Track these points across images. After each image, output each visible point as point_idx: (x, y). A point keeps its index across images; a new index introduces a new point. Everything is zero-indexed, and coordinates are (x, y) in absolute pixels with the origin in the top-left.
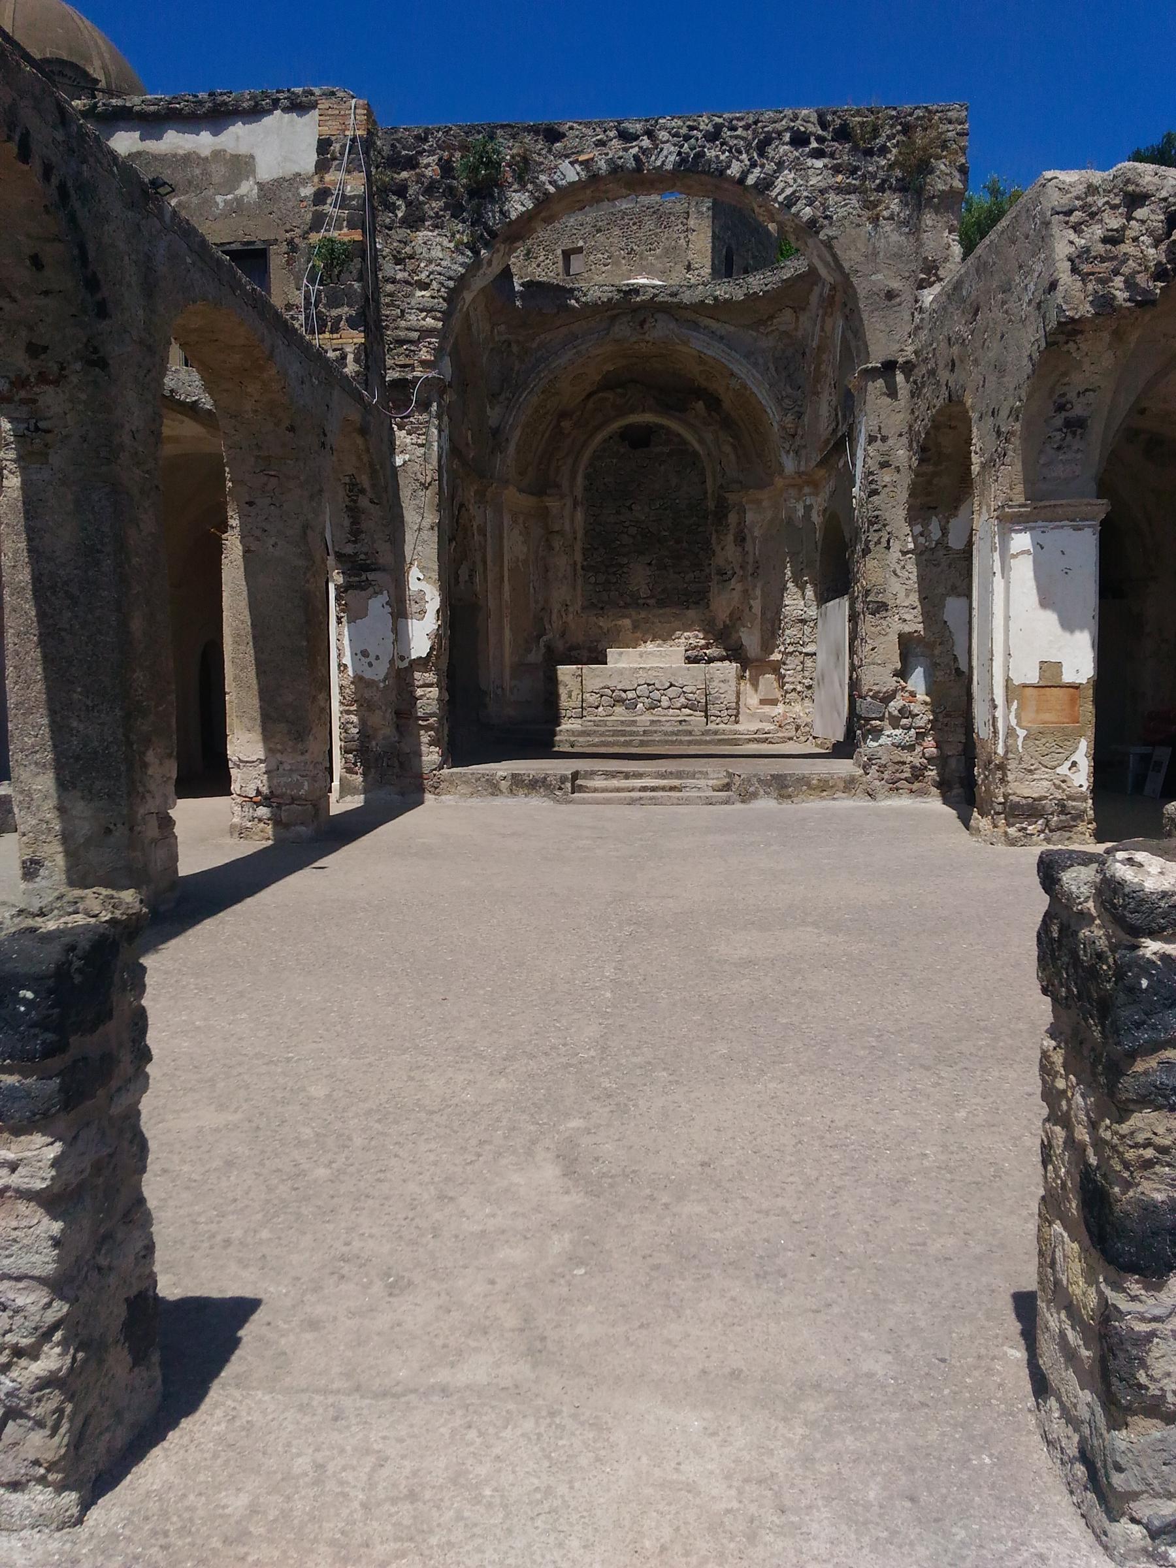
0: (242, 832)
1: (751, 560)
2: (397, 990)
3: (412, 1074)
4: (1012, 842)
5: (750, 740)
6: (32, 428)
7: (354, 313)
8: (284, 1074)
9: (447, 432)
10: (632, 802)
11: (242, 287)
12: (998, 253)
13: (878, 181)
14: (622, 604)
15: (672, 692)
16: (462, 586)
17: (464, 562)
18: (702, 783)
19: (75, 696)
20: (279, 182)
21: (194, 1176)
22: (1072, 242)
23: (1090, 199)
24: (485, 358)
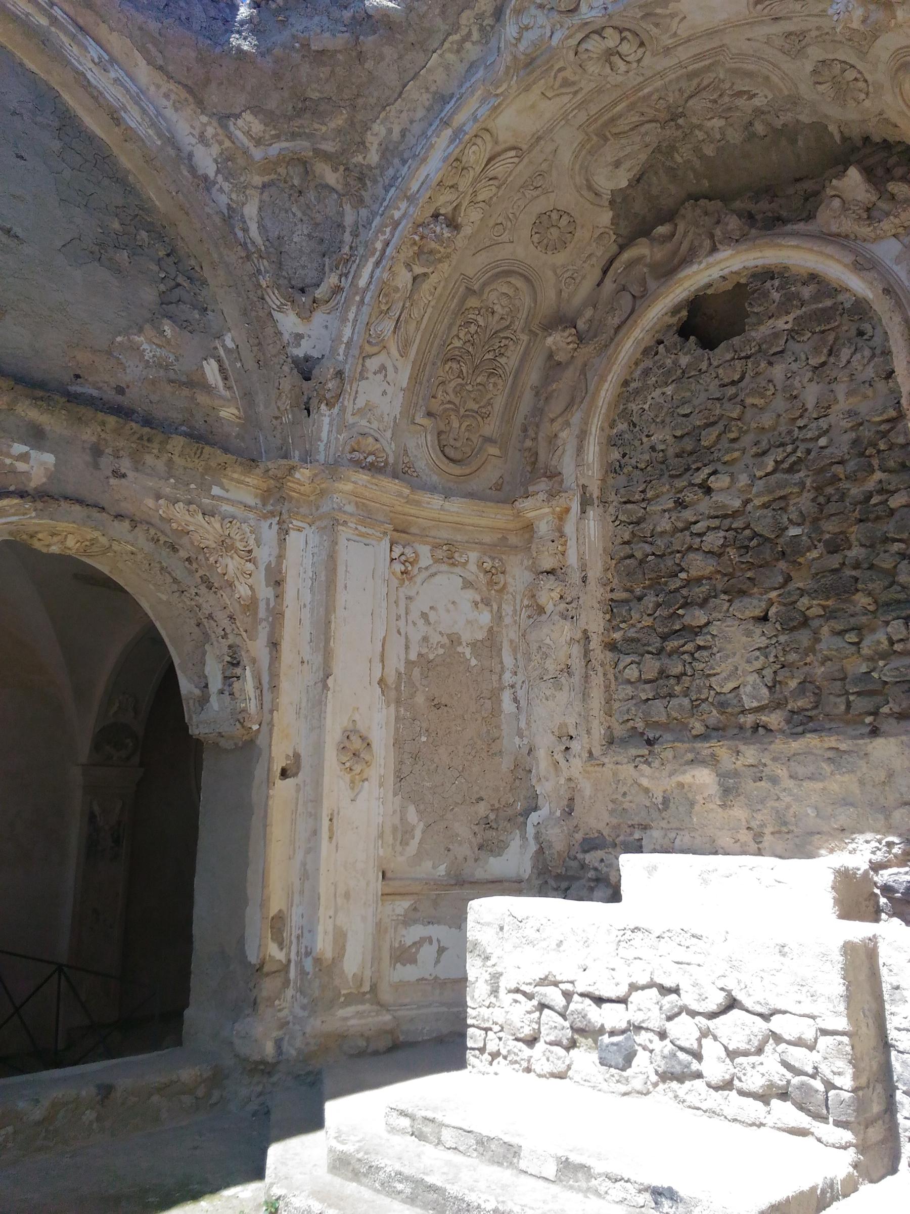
14: (699, 728)
17: (207, 647)
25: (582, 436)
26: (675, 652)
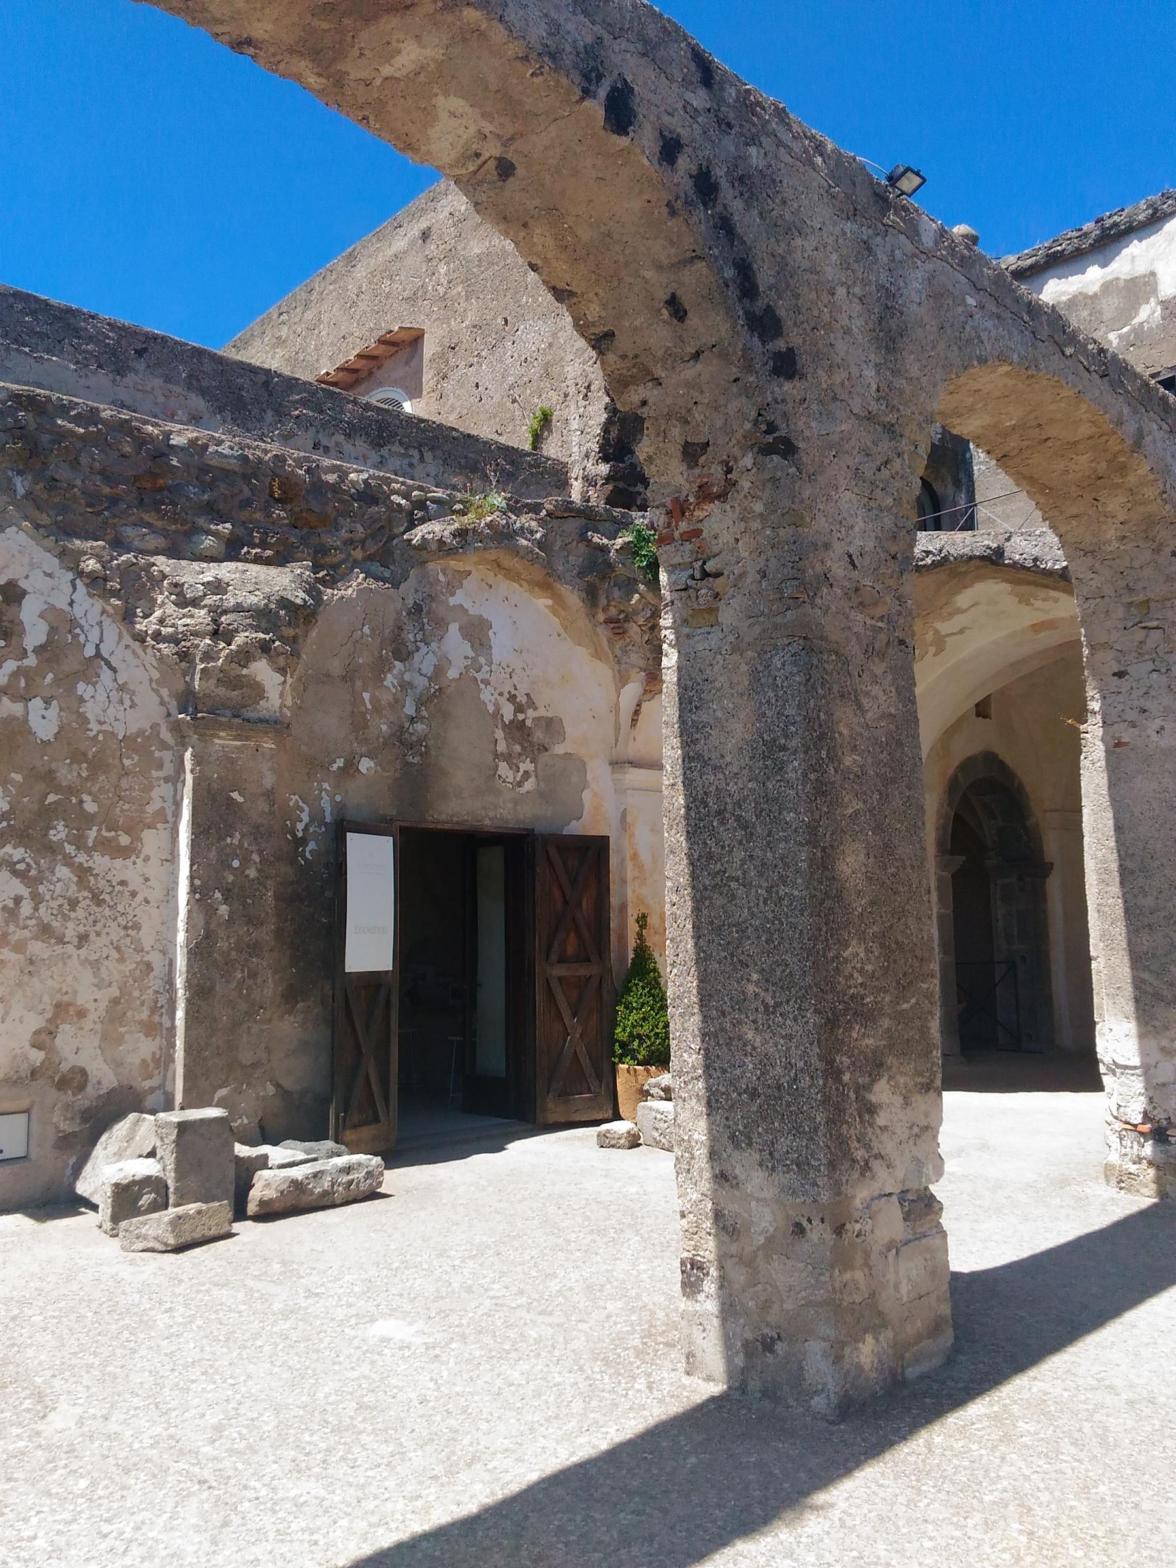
0: (1123, 1180)
6: (698, 575)
19: (751, 988)
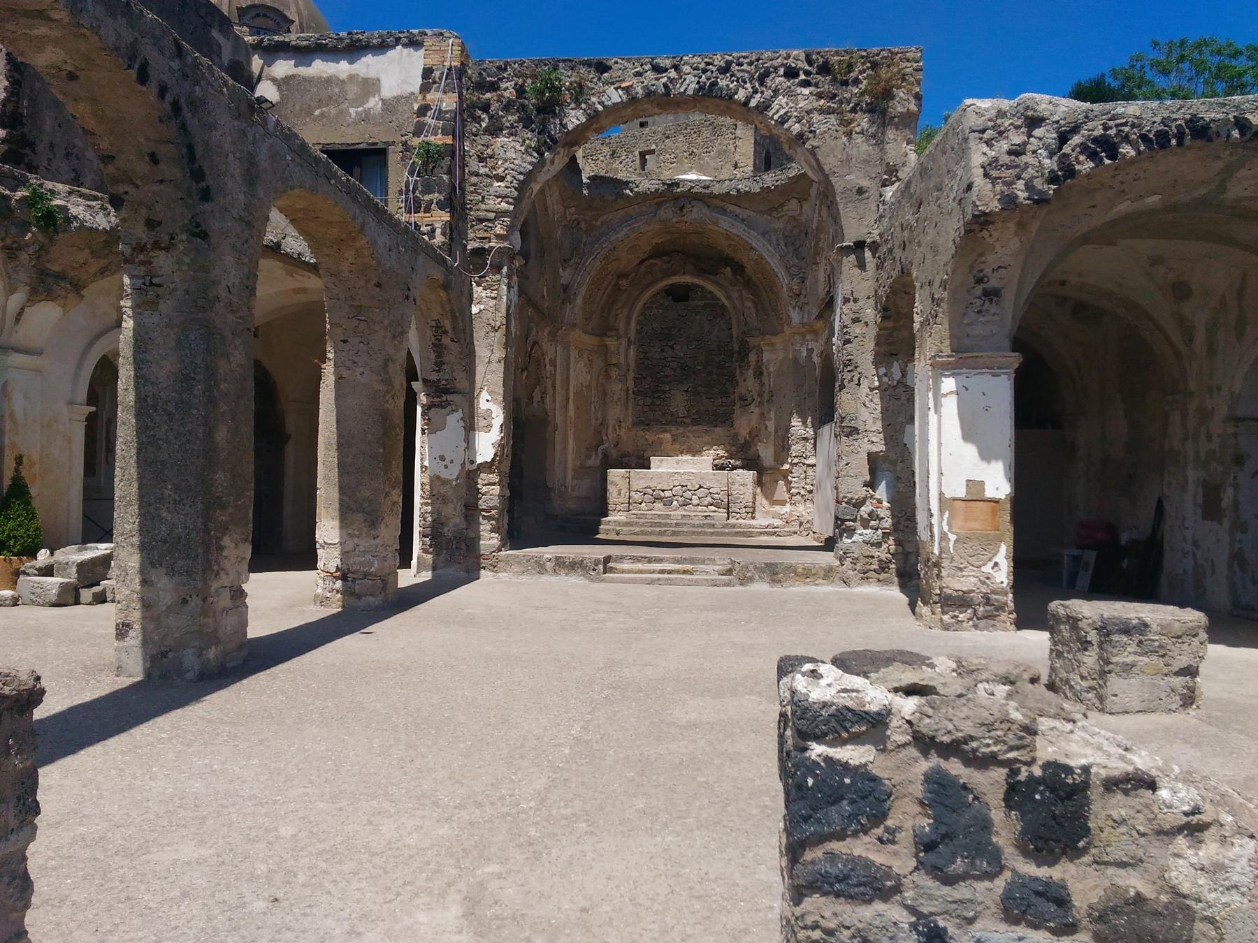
0: (323, 601)
1: (767, 391)
2: (392, 742)
3: (372, 819)
4: (946, 627)
5: (761, 533)
6: (147, 283)
7: (442, 198)
8: (266, 815)
9: (516, 288)
10: (652, 582)
11: (335, 175)
12: (934, 160)
13: (851, 105)
14: (664, 422)
15: (701, 492)
16: (535, 405)
18: (709, 568)
20: (398, 99)
21: (151, 905)
22: (985, 154)
23: (999, 121)
24: (559, 233)
25: (629, 318)
26: (659, 397)
